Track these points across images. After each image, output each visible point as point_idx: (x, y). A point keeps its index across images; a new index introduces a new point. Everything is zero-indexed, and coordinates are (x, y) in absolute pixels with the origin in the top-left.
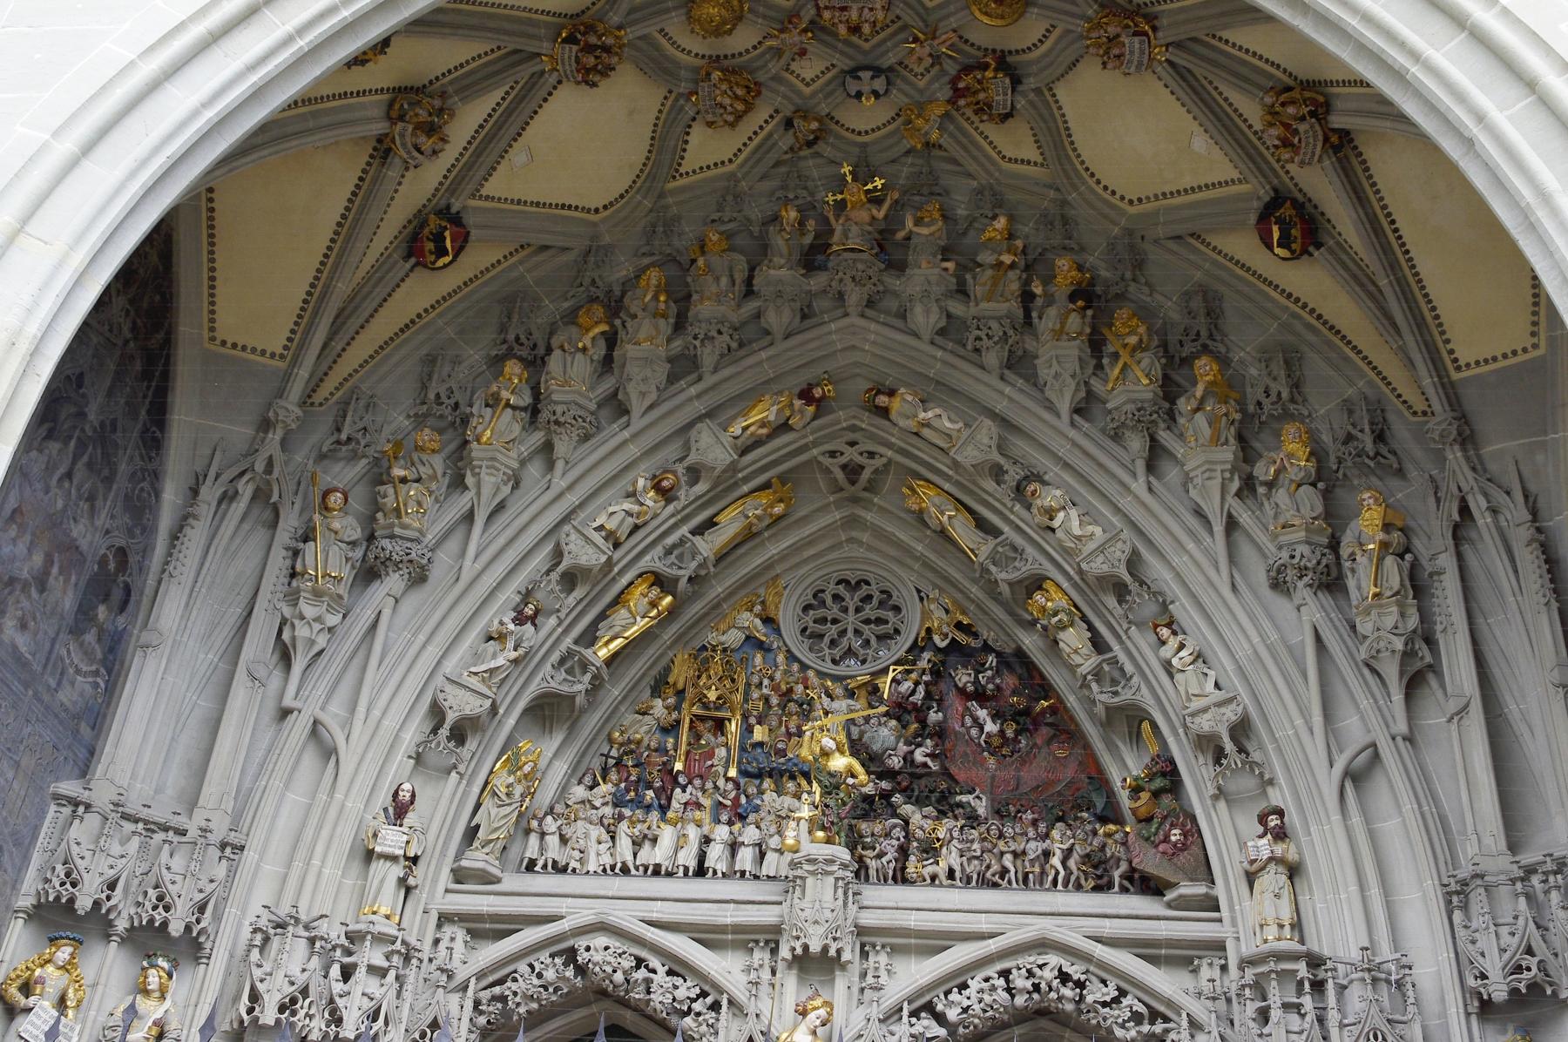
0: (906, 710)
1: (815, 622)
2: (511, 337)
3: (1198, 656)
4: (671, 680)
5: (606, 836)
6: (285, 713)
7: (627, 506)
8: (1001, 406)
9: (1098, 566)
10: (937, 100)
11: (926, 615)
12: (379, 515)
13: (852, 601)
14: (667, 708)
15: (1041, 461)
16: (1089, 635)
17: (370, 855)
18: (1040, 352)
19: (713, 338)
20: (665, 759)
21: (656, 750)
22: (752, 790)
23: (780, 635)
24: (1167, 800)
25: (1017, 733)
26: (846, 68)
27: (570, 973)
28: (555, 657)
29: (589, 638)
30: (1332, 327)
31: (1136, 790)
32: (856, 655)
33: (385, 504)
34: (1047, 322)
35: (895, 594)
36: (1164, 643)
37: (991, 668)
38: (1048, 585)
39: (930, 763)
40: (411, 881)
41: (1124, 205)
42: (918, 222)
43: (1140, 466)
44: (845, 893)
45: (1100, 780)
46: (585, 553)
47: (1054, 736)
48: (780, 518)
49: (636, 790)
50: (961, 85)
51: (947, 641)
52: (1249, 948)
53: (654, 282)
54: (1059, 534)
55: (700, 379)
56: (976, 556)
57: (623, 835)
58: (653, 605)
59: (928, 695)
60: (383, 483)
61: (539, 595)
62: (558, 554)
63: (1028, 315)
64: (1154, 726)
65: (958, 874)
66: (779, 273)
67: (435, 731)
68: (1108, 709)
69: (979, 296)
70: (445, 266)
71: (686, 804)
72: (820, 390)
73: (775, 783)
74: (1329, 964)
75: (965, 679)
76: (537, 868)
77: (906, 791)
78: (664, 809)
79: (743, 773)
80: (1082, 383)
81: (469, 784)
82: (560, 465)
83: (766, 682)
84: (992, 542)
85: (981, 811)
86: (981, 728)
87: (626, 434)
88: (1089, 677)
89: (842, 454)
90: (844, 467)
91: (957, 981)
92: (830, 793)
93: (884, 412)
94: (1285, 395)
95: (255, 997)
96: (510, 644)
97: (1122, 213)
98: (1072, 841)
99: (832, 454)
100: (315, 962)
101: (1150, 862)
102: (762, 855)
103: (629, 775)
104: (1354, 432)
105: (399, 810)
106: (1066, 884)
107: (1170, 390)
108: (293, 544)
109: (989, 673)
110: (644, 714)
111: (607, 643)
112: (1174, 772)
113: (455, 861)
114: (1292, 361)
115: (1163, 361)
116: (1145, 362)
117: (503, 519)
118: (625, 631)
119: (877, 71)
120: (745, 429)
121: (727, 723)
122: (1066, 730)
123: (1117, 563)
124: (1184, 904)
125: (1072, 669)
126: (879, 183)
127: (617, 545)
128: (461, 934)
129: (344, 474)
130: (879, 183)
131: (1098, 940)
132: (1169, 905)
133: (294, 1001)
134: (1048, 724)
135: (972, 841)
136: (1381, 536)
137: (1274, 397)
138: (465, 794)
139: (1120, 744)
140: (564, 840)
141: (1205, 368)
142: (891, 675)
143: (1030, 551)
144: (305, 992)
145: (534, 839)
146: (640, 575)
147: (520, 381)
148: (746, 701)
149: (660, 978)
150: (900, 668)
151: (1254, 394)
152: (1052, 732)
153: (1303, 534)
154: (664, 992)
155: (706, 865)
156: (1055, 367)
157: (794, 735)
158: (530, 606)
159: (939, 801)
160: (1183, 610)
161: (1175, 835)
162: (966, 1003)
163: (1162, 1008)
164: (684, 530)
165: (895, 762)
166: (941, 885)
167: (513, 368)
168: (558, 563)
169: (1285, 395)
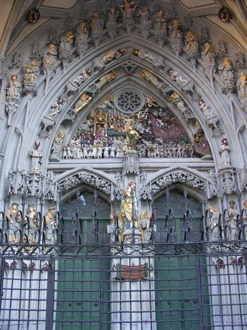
2: (51, 39)
3: (208, 108)
4: (91, 116)
6: (8, 127)
7: (81, 77)
8: (163, 53)
9: (186, 89)
11: (146, 100)
12: (25, 81)
13: (129, 97)
15: (172, 66)
17: (31, 157)
22: (111, 139)
23: (114, 105)
24: (201, 138)
25: (168, 125)
27: (77, 180)
28: (67, 112)
29: (74, 107)
31: (195, 136)
32: (131, 109)
34: (173, 35)
36: (200, 105)
38: (174, 93)
40: (41, 162)
42: (142, 12)
43: (194, 66)
45: (185, 134)
46: (72, 88)
48: (114, 79)
52: (220, 167)
53: (83, 26)
54: (177, 81)
55: (95, 48)
58: (87, 99)
59: (148, 118)
60: (25, 74)
61: (62, 98)
62: (66, 88)
63: (168, 33)
64: (198, 122)
65: (159, 155)
66: (111, 23)
67: (42, 129)
68: (189, 119)
70: (35, 22)
74: (237, 170)
77: (146, 139)
78: (92, 144)
79: (108, 135)
81: (51, 140)
82: (65, 68)
83: (112, 116)
84: (162, 84)
85: (161, 142)
86: (160, 124)
87: (79, 60)
90: (127, 67)
91: (161, 177)
93: (137, 55)
95: (12, 188)
99: (125, 64)
100: (24, 180)
101: (198, 151)
102: (115, 153)
104: (239, 60)
105: (37, 147)
106: (181, 156)
107: (200, 50)
108: (6, 88)
112: (203, 133)
114: (225, 44)
116: (195, 44)
117: (53, 80)
122: (178, 124)
124: (206, 159)
125: (180, 111)
126: (133, 3)
127: (79, 86)
128: (52, 173)
129: (15, 72)
131: (190, 167)
132: (203, 159)
133: (20, 188)
136: (245, 82)
138: (50, 143)
139: (190, 126)
140: (72, 152)
143: (170, 85)
144: (22, 187)
145: (65, 152)
148: (108, 120)
149: (97, 180)
151: (217, 51)
153: (229, 82)
154: (98, 183)
160: (204, 98)
161: (204, 145)
162: (163, 181)
163: (202, 180)
164: (93, 82)
165: (142, 132)
168: (66, 90)
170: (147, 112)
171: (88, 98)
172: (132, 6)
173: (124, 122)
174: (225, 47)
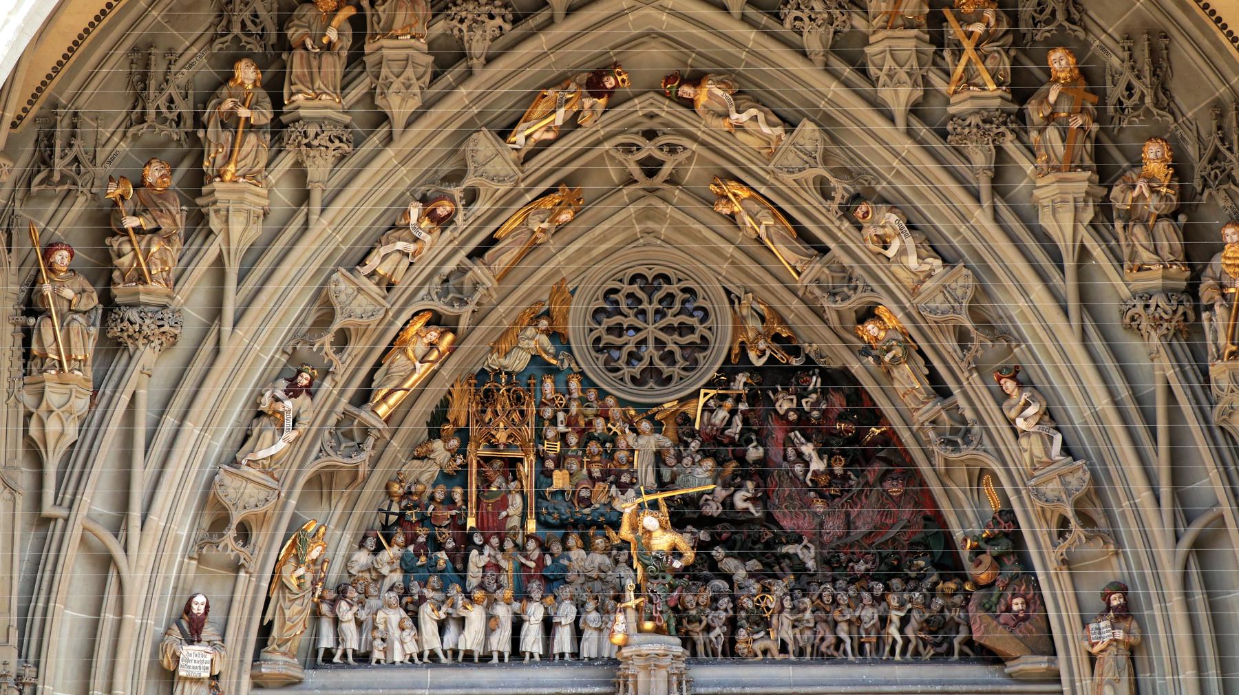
0: (721, 443)
1: (609, 330)
4: (451, 417)
5: (408, 623)
12: (116, 274)
14: (449, 450)
16: (927, 372)
18: (872, 39)
19: (483, 22)
20: (454, 512)
21: (442, 502)
22: (557, 548)
23: (570, 351)
28: (333, 420)
32: (660, 372)
33: (123, 264)
35: (700, 293)
37: (815, 391)
38: (881, 311)
39: (752, 510)
43: (984, 186)
44: (680, 684)
45: (937, 518)
48: (567, 223)
49: (426, 555)
51: (764, 359)
55: (469, 73)
56: (799, 274)
57: (427, 618)
59: (745, 421)
60: (113, 234)
65: (791, 647)
71: (484, 567)
72: (612, 80)
73: (583, 537)
75: (786, 406)
76: (336, 659)
77: (729, 544)
79: (541, 523)
81: (259, 579)
85: (810, 564)
86: (807, 464)
88: (926, 424)
90: (640, 163)
92: (656, 578)
94: (1148, 100)
96: (288, 424)
98: (909, 606)
99: (628, 148)
103: (417, 536)
104: (1222, 149)
106: (904, 652)
109: (814, 396)
111: (385, 398)
112: (1016, 538)
113: (253, 667)
120: (528, 137)
121: (519, 464)
123: (956, 305)
134: (881, 459)
135: (805, 610)
137: (1136, 97)
140: (359, 624)
141: (1060, 61)
142: (702, 400)
146: (416, 314)
150: (712, 393)
151: (1115, 92)
155: (523, 648)
156: (889, 63)
157: (599, 480)
158: (305, 375)
161: (1017, 605)
164: (463, 254)
165: (713, 509)
166: (774, 662)
167: (246, 73)
169: (1148, 100)
170: (738, 399)
171: (442, 335)
173: (622, 455)
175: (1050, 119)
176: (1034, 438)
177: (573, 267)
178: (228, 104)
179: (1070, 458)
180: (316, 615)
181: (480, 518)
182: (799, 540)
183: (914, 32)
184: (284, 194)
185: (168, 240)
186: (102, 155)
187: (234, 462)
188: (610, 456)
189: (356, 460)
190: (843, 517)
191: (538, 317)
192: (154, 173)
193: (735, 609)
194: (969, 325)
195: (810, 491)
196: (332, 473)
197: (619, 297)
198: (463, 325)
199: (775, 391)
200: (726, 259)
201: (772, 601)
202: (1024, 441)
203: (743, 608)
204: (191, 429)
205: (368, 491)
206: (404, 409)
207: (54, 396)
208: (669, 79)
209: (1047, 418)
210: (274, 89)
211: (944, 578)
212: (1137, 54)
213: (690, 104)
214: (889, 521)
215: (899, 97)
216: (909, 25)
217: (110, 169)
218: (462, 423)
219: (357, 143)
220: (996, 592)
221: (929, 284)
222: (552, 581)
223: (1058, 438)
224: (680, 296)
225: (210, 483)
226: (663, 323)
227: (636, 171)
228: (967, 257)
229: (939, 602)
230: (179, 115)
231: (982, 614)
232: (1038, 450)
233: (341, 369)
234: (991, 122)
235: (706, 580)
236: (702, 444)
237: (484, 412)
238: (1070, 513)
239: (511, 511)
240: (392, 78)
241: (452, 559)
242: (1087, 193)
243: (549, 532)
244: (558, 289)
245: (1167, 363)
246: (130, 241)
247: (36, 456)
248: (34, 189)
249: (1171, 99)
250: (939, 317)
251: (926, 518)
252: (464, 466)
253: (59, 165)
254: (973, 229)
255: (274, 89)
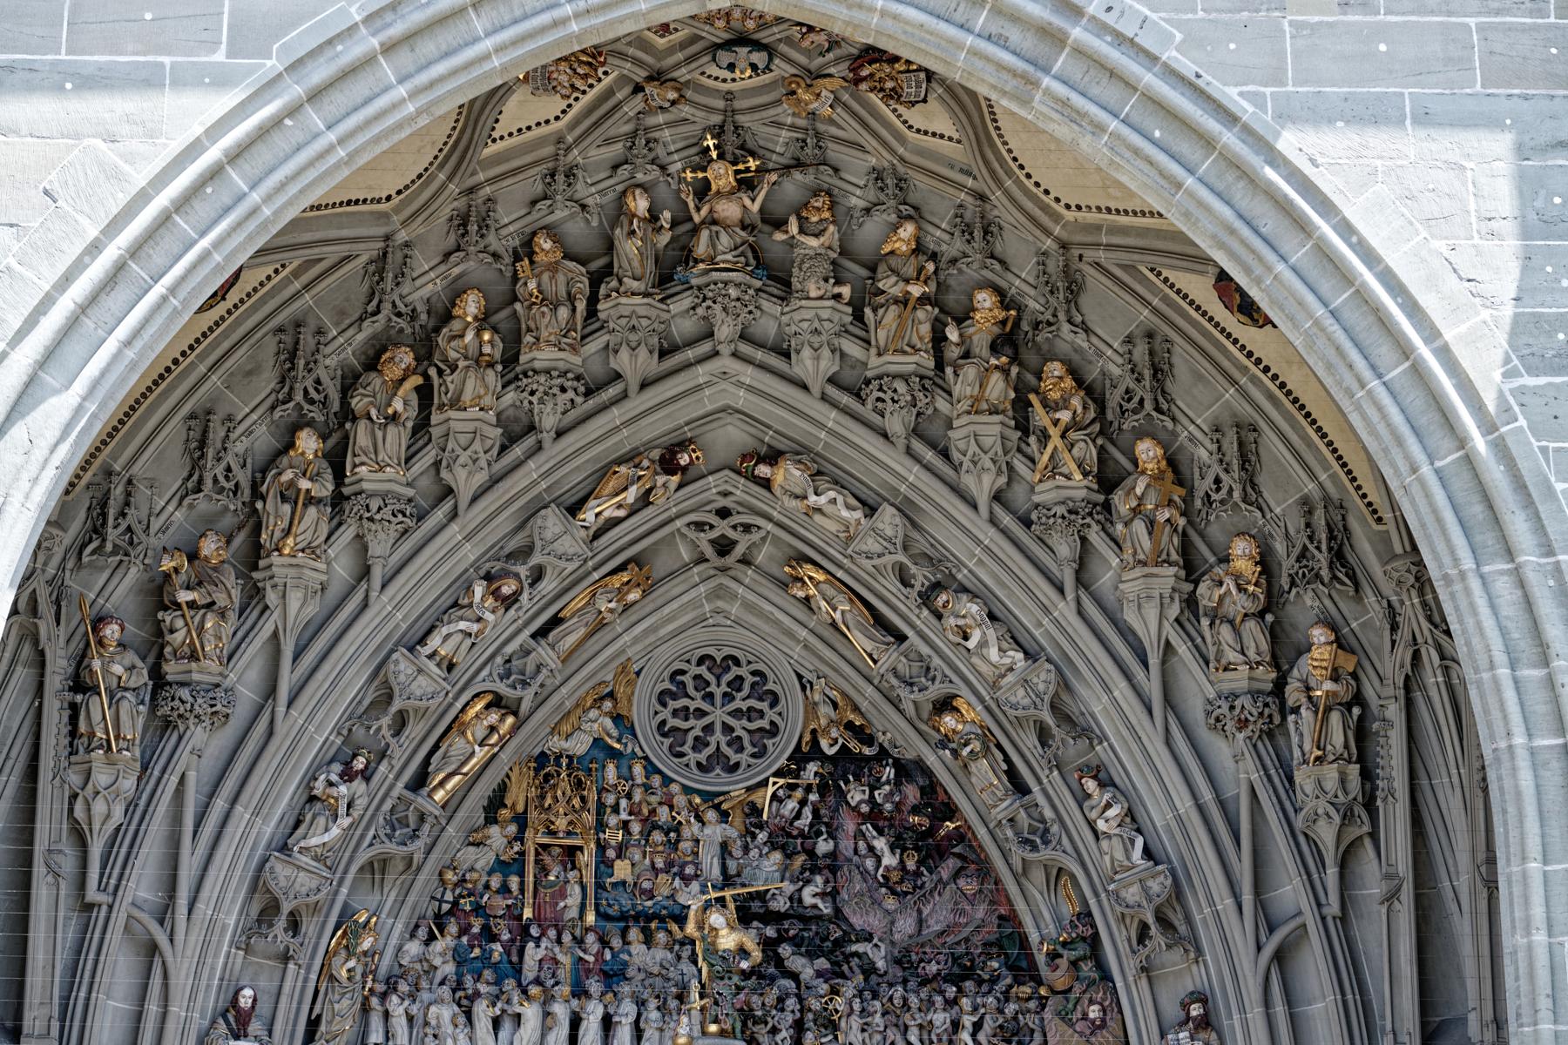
0: (789, 835)
1: (675, 713)
3: (1130, 813)
4: (508, 802)
5: (462, 1020)
10: (830, 76)
11: (810, 709)
12: (168, 650)
16: (1005, 767)
20: (510, 902)
21: (498, 892)
22: (616, 943)
23: (635, 735)
25: (920, 863)
26: (718, 41)
28: (387, 806)
30: (1295, 401)
34: (965, 382)
37: (888, 782)
38: (958, 703)
39: (821, 905)
41: (1060, 209)
45: (1010, 919)
47: (962, 868)
50: (864, 73)
55: (539, 447)
56: (875, 662)
60: (166, 608)
69: (882, 343)
71: (540, 961)
72: (686, 457)
77: (797, 942)
78: (517, 971)
80: (1004, 468)
85: (881, 964)
86: (879, 860)
89: (712, 527)
90: (712, 542)
92: (722, 978)
94: (1236, 495)
96: (342, 810)
97: (1057, 217)
98: (982, 1011)
99: (700, 526)
103: (470, 926)
107: (1108, 480)
109: (887, 788)
110: (477, 844)
111: (442, 784)
112: (1094, 941)
115: (1100, 441)
118: (463, 764)
119: (758, 46)
120: (597, 515)
123: (1038, 701)
130: (753, 164)
136: (1329, 686)
137: (1224, 491)
138: (306, 980)
140: (410, 1019)
141: (1147, 451)
142: (771, 790)
145: (376, 1021)
146: (477, 695)
147: (316, 456)
150: (781, 781)
151: (1203, 486)
152: (959, 864)
156: (973, 448)
159: (832, 952)
161: (1094, 1012)
165: (780, 905)
167: (308, 443)
169: (1236, 495)
170: (808, 789)
171: (502, 719)
172: (746, 184)
173: (685, 846)
174: (1244, 460)
175: (1136, 511)
176: (1115, 840)
177: (639, 647)
178: (288, 476)
179: (1151, 863)
180: (366, 1009)
181: (537, 908)
182: (868, 938)
183: (997, 418)
184: (342, 568)
185: (222, 614)
186: (156, 525)
187: (284, 848)
188: (674, 846)
189: (411, 847)
190: (915, 914)
191: (602, 699)
192: (209, 547)
193: (801, 1011)
194: (1049, 720)
195: (881, 885)
196: (385, 861)
197: (687, 679)
198: (525, 707)
199: (847, 782)
200: (799, 641)
201: (840, 1003)
202: (1104, 844)
203: (810, 1010)
204: (242, 813)
205: (422, 877)
206: (461, 794)
207: (101, 777)
208: (744, 457)
209: (1128, 820)
210: (336, 460)
211: (1018, 981)
212: (1225, 446)
213: (766, 484)
214: (963, 920)
215: (982, 485)
216: (994, 411)
217: (165, 539)
218: (520, 808)
219: (421, 518)
220: (1072, 996)
221: (1010, 678)
222: (611, 976)
223: (1140, 842)
224: (750, 679)
225: (261, 868)
226: (731, 707)
227: (709, 552)
228: (1049, 650)
229: (1011, 1008)
230: (237, 485)
231: (1057, 1020)
232: (1119, 855)
233: (397, 754)
234: (1077, 513)
235: (773, 979)
236: (770, 835)
237: (542, 797)
238: (1150, 920)
239: (569, 901)
240: (459, 451)
241: (508, 953)
242: (1174, 589)
243: (609, 925)
244: (624, 668)
245: (1251, 767)
246: (183, 616)
247: (80, 839)
248: (85, 559)
249: (1259, 493)
250: (1020, 713)
251: (1001, 917)
252: (522, 853)
253: (112, 534)
254: (1056, 622)
255: (336, 460)
